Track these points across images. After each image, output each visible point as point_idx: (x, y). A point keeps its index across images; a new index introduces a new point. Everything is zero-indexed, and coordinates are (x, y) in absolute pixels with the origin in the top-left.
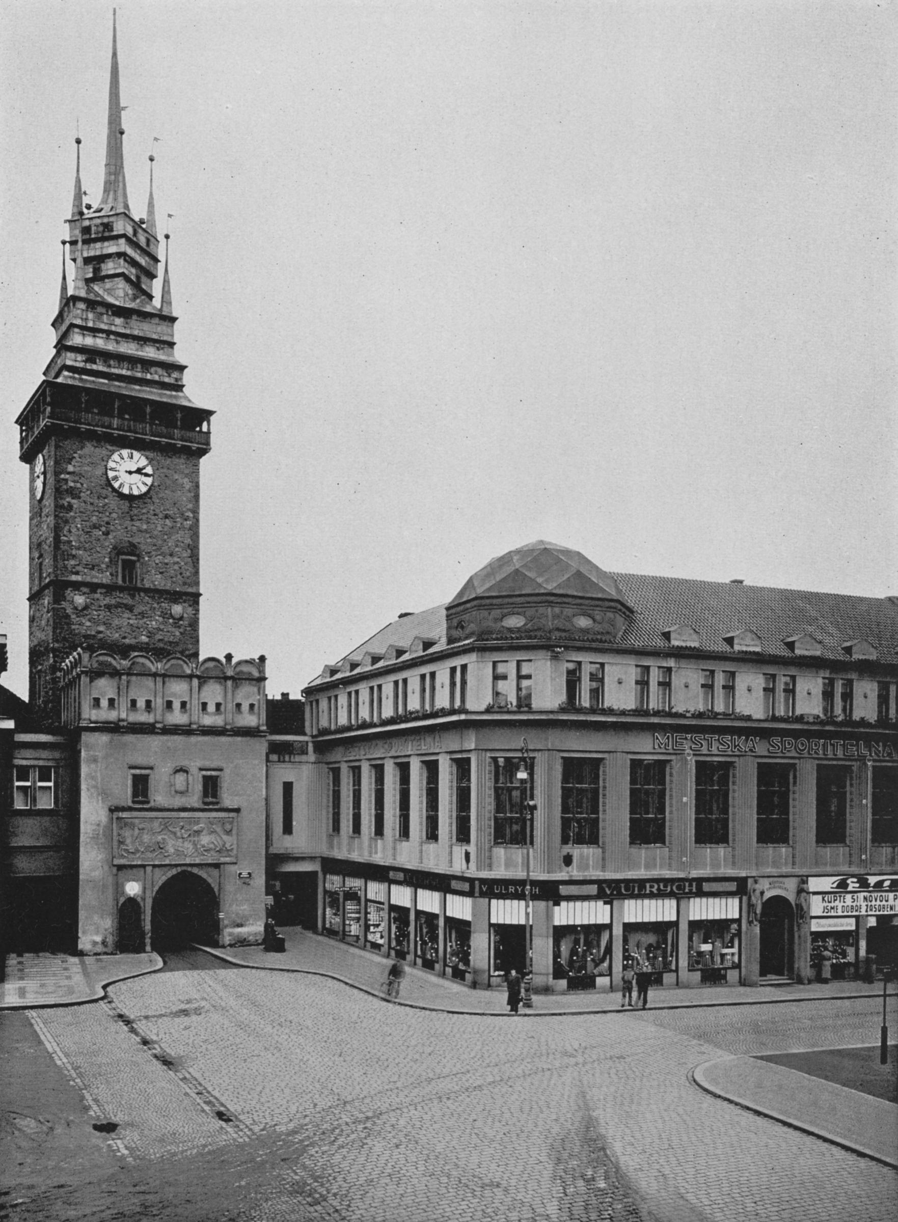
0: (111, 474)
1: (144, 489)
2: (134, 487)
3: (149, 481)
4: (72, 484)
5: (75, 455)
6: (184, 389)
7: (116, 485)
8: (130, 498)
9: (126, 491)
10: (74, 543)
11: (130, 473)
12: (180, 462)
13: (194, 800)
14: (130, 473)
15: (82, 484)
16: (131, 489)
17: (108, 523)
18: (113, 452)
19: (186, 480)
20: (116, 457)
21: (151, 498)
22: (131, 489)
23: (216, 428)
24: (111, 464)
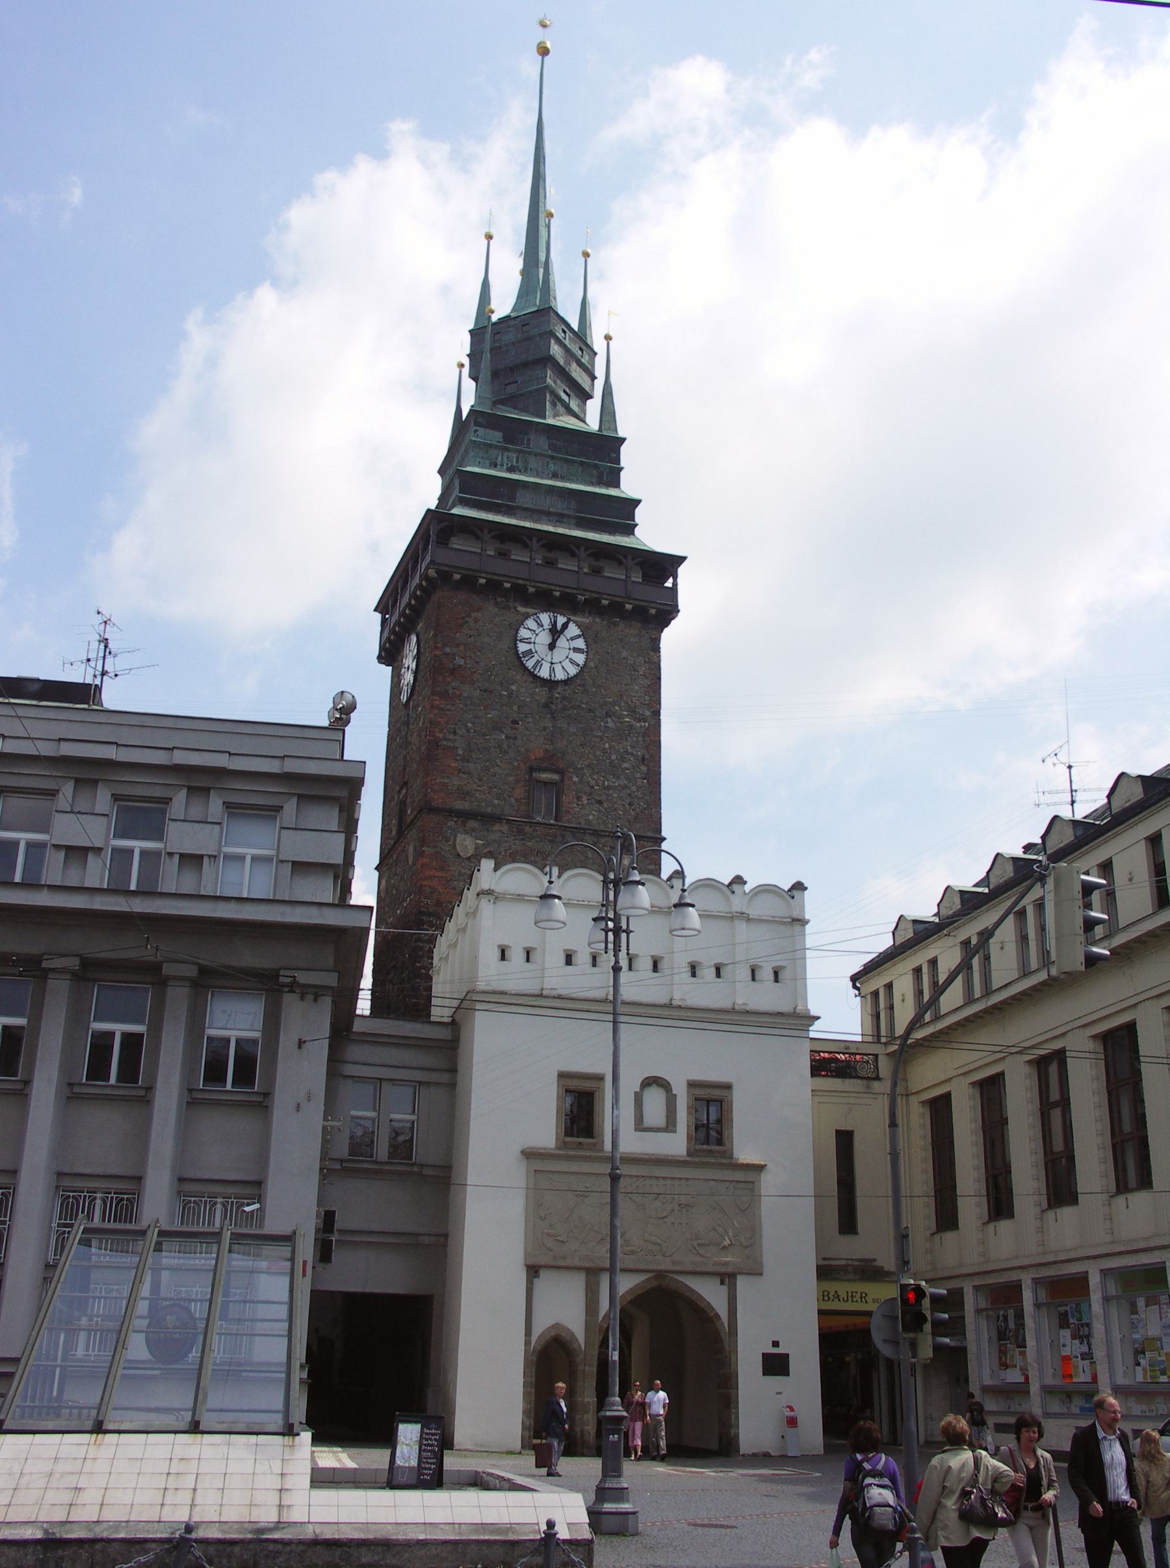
0: (522, 647)
1: (573, 671)
2: (558, 668)
3: (580, 658)
4: (462, 662)
5: (467, 619)
6: (637, 530)
7: (530, 664)
8: (551, 684)
9: (544, 673)
10: (460, 752)
11: (552, 646)
12: (631, 631)
13: (676, 1144)
14: (552, 646)
15: (477, 663)
16: (552, 670)
17: (515, 722)
18: (527, 616)
19: (641, 660)
20: (530, 623)
21: (583, 685)
22: (552, 670)
23: (687, 582)
24: (523, 633)
